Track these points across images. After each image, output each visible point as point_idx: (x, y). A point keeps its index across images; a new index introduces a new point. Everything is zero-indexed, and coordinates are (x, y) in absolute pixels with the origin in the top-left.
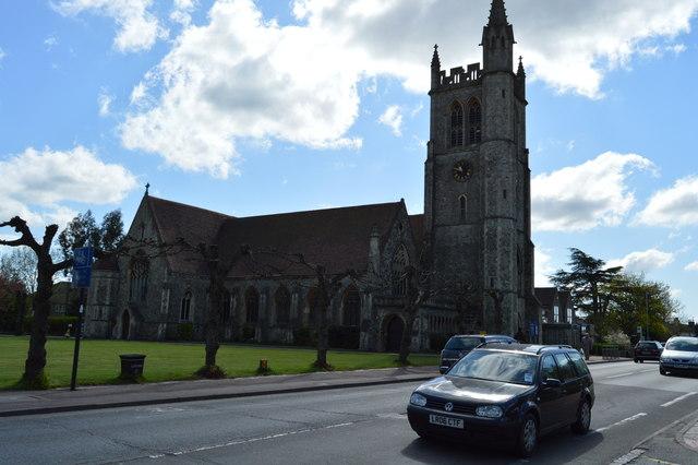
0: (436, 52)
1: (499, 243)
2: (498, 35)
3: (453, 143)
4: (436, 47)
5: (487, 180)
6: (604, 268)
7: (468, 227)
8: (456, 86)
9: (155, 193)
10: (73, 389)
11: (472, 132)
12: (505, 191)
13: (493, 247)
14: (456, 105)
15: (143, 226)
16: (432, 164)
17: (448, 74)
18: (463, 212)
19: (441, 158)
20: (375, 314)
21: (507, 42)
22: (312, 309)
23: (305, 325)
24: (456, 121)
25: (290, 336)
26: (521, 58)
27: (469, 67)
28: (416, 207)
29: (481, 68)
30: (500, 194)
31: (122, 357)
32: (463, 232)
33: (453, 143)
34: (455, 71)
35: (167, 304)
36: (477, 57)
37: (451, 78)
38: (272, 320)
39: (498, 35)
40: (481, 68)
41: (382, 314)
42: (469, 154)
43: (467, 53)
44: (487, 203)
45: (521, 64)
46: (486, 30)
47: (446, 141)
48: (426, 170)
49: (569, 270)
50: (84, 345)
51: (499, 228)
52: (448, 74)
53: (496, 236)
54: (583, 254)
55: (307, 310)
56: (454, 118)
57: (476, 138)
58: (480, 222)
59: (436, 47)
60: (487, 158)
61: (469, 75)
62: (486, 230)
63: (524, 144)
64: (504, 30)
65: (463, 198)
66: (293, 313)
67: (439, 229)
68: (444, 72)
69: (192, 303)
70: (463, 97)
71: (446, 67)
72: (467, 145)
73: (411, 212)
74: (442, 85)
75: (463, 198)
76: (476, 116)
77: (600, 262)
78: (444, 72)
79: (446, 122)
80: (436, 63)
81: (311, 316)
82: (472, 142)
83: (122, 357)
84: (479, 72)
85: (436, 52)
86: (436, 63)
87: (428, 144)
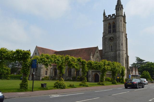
0: (104, 11)
1: (121, 56)
2: (119, 7)
3: (109, 33)
4: (104, 10)
5: (117, 41)
6: (145, 62)
7: (113, 52)
8: (110, 19)
9: (39, 46)
10: (32, 91)
11: (113, 30)
12: (122, 44)
13: (119, 57)
14: (110, 24)
15: (36, 53)
16: (104, 38)
17: (107, 17)
18: (112, 49)
19: (106, 36)
20: (92, 73)
21: (122, 9)
22: (76, 72)
23: (75, 76)
24: (110, 27)
25: (71, 79)
26: (124, 12)
27: (112, 14)
28: (100, 48)
29: (115, 15)
30: (121, 45)
31: (41, 84)
32: (112, 54)
33: (109, 33)
35: (42, 72)
36: (114, 12)
37: (108, 17)
38: (67, 75)
39: (119, 7)
40: (115, 15)
41: (94, 73)
42: (113, 35)
43: (111, 11)
44: (118, 47)
45: (124, 14)
46: (116, 6)
47: (107, 32)
48: (103, 39)
49: (136, 62)
50: (34, 81)
51: (121, 53)
52: (107, 17)
53: (120, 54)
54: (139, 58)
55: (75, 73)
56: (109, 27)
57: (115, 31)
58: (116, 51)
59: (104, 10)
60: (117, 36)
61: (112, 16)
62: (118, 53)
63: (126, 33)
64: (120, 6)
65: (112, 46)
66: (72, 73)
67: (106, 53)
68: (106, 16)
69: (48, 72)
70: (111, 22)
71: (107, 15)
72: (112, 33)
73: (99, 49)
74: (106, 19)
75: (112, 46)
76: (114, 26)
77: (144, 60)
78: (106, 16)
79: (107, 28)
80: (104, 14)
81: (76, 74)
82: (113, 32)
83: (41, 84)
84: (115, 16)
85: (104, 11)
86: (104, 14)
87: (103, 33)
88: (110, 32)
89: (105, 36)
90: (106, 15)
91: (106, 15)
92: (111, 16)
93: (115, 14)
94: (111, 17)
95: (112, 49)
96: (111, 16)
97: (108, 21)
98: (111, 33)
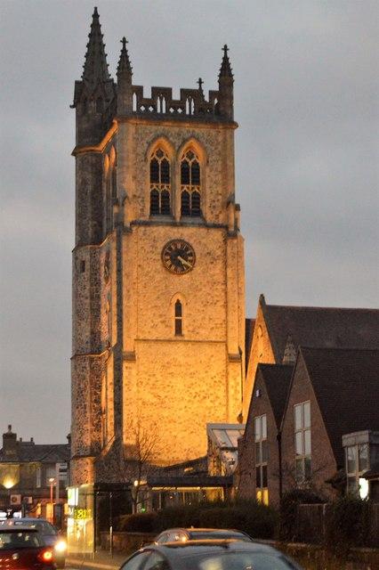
3: (154, 210)
4: (124, 41)
11: (185, 196)
17: (147, 94)
18: (179, 325)
24: (159, 171)
34: (157, 91)
37: (152, 102)
52: (147, 94)
56: (154, 165)
57: (192, 208)
61: (181, 104)
68: (139, 90)
71: (144, 78)
76: (191, 174)
78: (139, 90)
88: (160, 206)
89: (133, 223)
90: (135, 81)
91: (135, 81)
92: (176, 96)
93: (195, 95)
94: (171, 104)
95: (179, 325)
96: (176, 96)
97: (153, 129)
98: (167, 210)
